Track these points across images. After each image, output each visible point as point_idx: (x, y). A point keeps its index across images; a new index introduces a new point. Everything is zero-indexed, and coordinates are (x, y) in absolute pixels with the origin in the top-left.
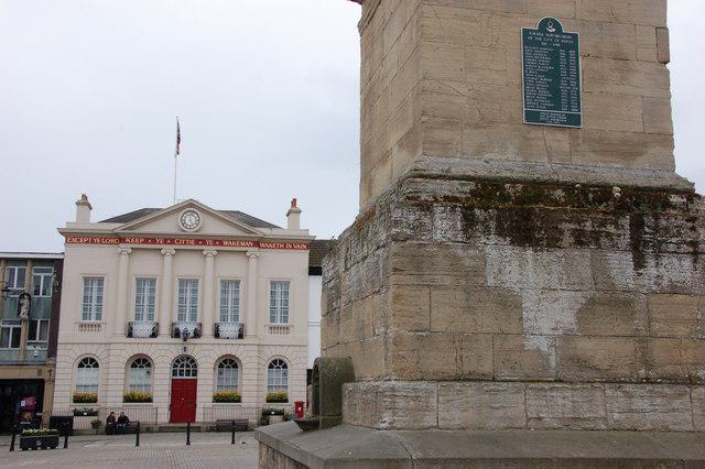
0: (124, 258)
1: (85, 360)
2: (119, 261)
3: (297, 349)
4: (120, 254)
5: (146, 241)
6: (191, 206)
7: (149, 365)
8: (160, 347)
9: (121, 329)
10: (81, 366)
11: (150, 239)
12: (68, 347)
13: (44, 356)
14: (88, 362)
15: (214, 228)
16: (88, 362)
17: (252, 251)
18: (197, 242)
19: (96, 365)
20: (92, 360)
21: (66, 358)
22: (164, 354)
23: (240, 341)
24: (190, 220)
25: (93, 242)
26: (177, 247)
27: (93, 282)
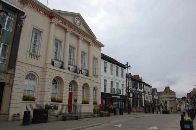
0: (53, 26)
1: (29, 75)
2: (50, 26)
3: (99, 84)
4: (51, 23)
5: (62, 22)
6: (79, 16)
7: (56, 84)
8: (67, 75)
9: (50, 62)
10: (27, 78)
11: (65, 22)
12: (23, 65)
13: (3, 68)
14: (31, 76)
15: (82, 28)
16: (31, 76)
17: (92, 43)
18: (78, 32)
19: (34, 79)
20: (33, 75)
21: (21, 70)
22: (67, 77)
23: (86, 77)
24: (78, 22)
25: (39, 11)
26: (73, 31)
27: (37, 33)
